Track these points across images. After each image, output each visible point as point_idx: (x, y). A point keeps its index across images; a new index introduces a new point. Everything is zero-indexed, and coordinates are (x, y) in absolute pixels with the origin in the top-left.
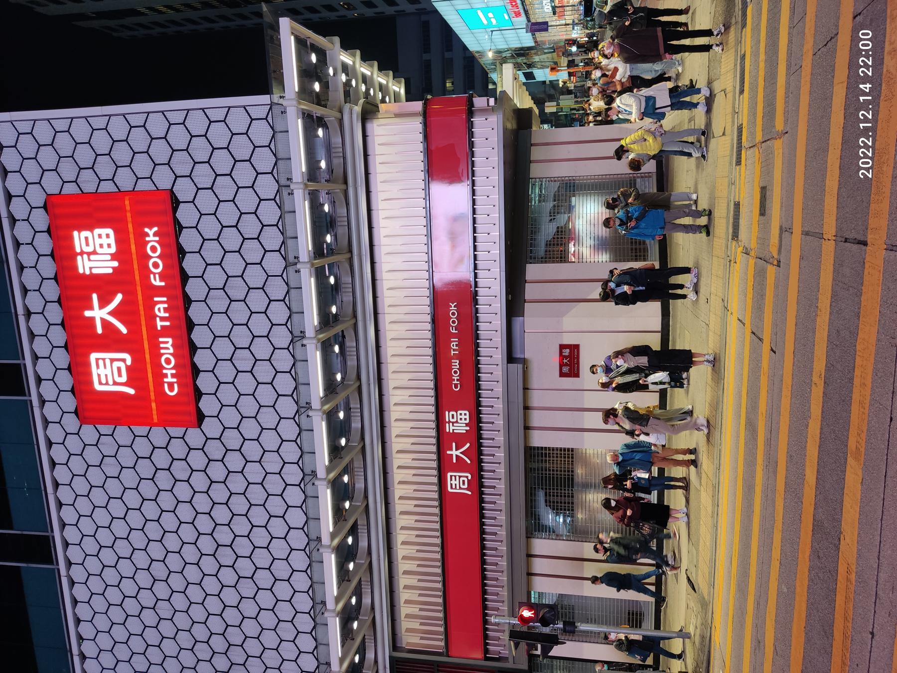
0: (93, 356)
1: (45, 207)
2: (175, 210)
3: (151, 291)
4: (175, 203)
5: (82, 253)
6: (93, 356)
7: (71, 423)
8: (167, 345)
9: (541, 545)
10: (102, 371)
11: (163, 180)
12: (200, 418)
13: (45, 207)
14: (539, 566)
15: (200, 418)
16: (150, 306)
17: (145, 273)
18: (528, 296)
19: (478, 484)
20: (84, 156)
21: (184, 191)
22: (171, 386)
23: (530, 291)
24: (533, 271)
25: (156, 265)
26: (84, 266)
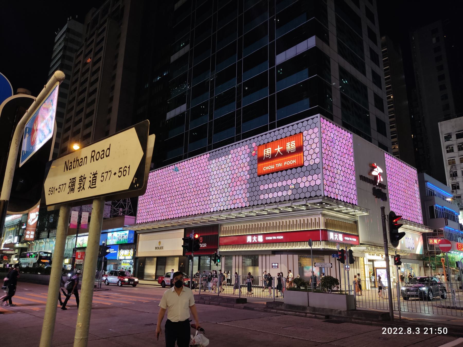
0: (270, 148)
1: (300, 132)
2: (300, 167)
3: (283, 162)
4: (302, 166)
5: (291, 143)
6: (270, 148)
7: (258, 144)
8: (272, 167)
9: (241, 258)
10: (268, 151)
11: (306, 164)
12: (259, 176)
13: (300, 132)
14: (237, 258)
15: (259, 176)
16: (280, 162)
17: (286, 161)
18: (294, 255)
19: (249, 244)
20: (311, 142)
21: (304, 169)
22: (265, 169)
23: (290, 256)
24: (296, 257)
25: (288, 163)
26: (288, 144)
